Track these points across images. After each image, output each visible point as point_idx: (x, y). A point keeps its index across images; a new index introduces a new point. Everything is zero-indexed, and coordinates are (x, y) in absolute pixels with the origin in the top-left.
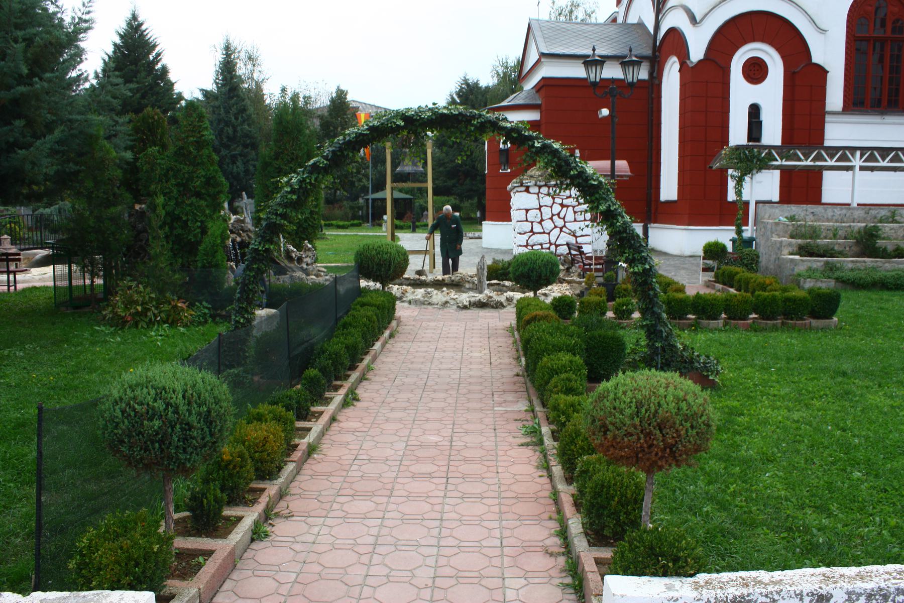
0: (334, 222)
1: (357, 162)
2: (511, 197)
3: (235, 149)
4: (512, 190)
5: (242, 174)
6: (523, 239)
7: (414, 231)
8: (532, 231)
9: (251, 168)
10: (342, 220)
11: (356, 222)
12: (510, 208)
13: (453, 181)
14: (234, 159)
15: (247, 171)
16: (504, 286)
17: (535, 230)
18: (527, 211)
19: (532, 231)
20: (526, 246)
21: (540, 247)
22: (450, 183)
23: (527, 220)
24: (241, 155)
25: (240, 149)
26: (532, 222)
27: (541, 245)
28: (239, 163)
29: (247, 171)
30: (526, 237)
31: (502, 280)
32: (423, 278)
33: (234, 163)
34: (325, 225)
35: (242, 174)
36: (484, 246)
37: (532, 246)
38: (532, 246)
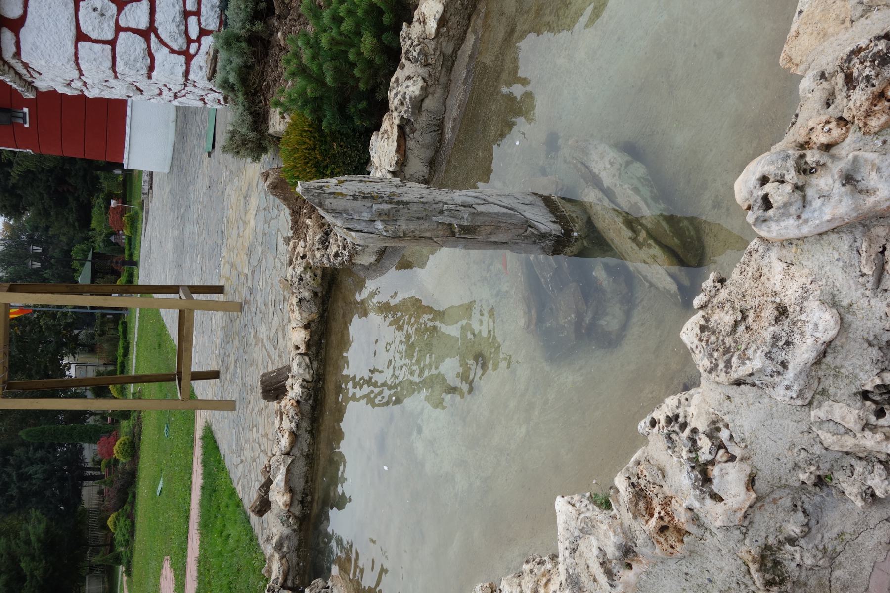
0: (119, 360)
1: (38, 318)
2: (53, 93)
3: (9, 476)
4: (29, 85)
5: (47, 467)
6: (169, 66)
7: (136, 264)
8: (145, 34)
9: (39, 454)
10: (116, 346)
11: (120, 329)
12: (82, 98)
13: (71, 199)
14: (23, 477)
15: (42, 461)
16: (418, 104)
17: (143, 24)
18: (81, 37)
19: (145, 34)
20: (189, 58)
21: (193, 20)
22: (73, 204)
23: (112, 43)
24: (19, 468)
25: (9, 469)
26: (118, 29)
27: (186, 14)
28: (31, 470)
29: (42, 461)
30: (161, 54)
31: (383, 107)
32: (295, 391)
33: (29, 478)
34: (122, 372)
35: (47, 467)
36: (167, 170)
37: (189, 41)
38: (189, 41)
